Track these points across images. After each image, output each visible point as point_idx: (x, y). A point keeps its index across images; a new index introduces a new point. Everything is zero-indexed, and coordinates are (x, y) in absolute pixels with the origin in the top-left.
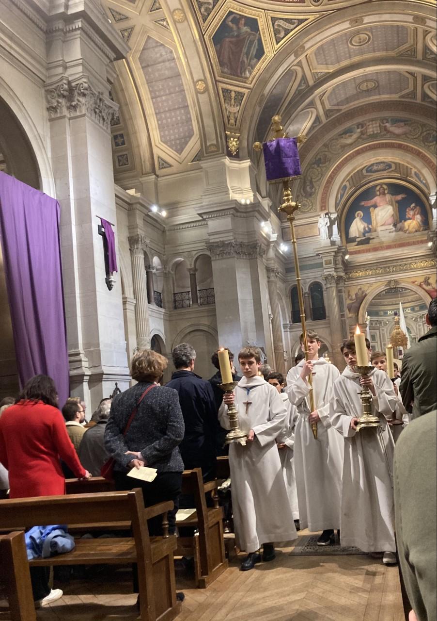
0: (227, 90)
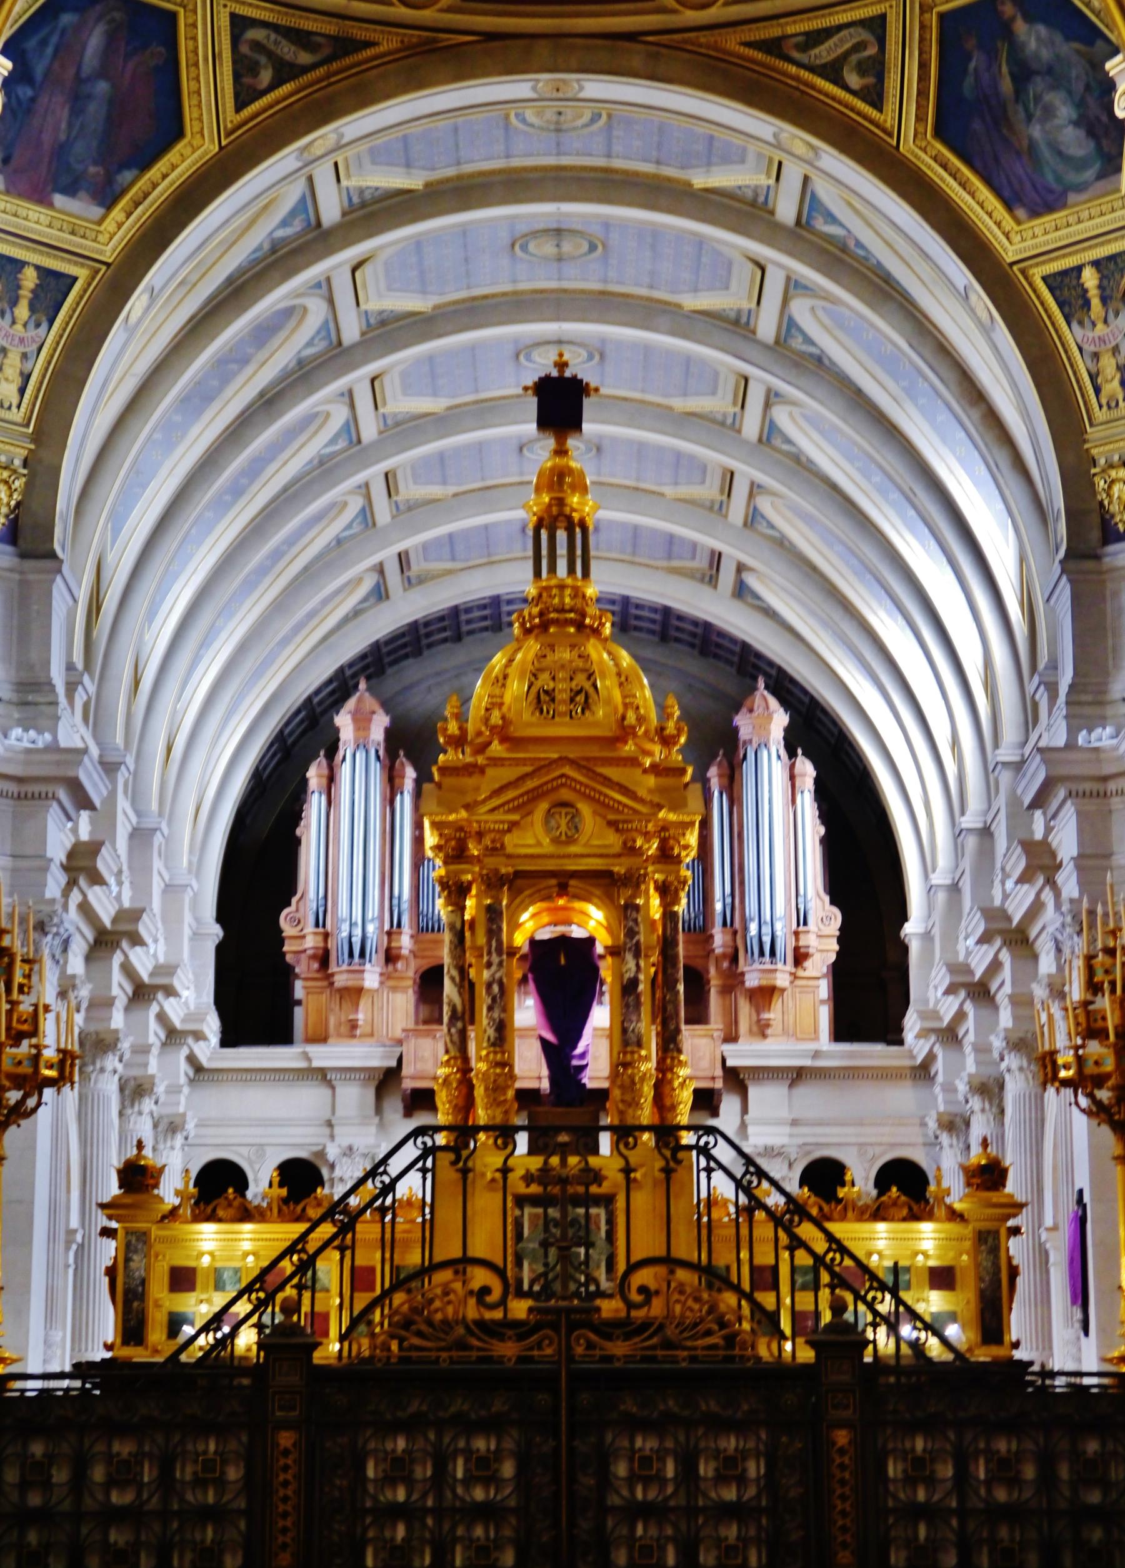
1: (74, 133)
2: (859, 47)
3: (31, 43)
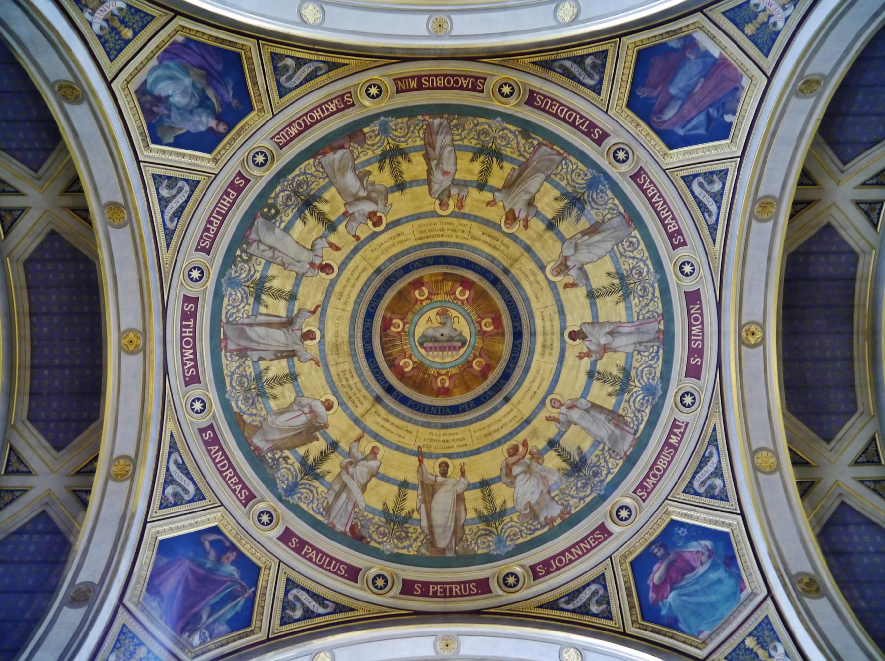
1: (696, 78)
2: (289, 78)
3: (702, 131)
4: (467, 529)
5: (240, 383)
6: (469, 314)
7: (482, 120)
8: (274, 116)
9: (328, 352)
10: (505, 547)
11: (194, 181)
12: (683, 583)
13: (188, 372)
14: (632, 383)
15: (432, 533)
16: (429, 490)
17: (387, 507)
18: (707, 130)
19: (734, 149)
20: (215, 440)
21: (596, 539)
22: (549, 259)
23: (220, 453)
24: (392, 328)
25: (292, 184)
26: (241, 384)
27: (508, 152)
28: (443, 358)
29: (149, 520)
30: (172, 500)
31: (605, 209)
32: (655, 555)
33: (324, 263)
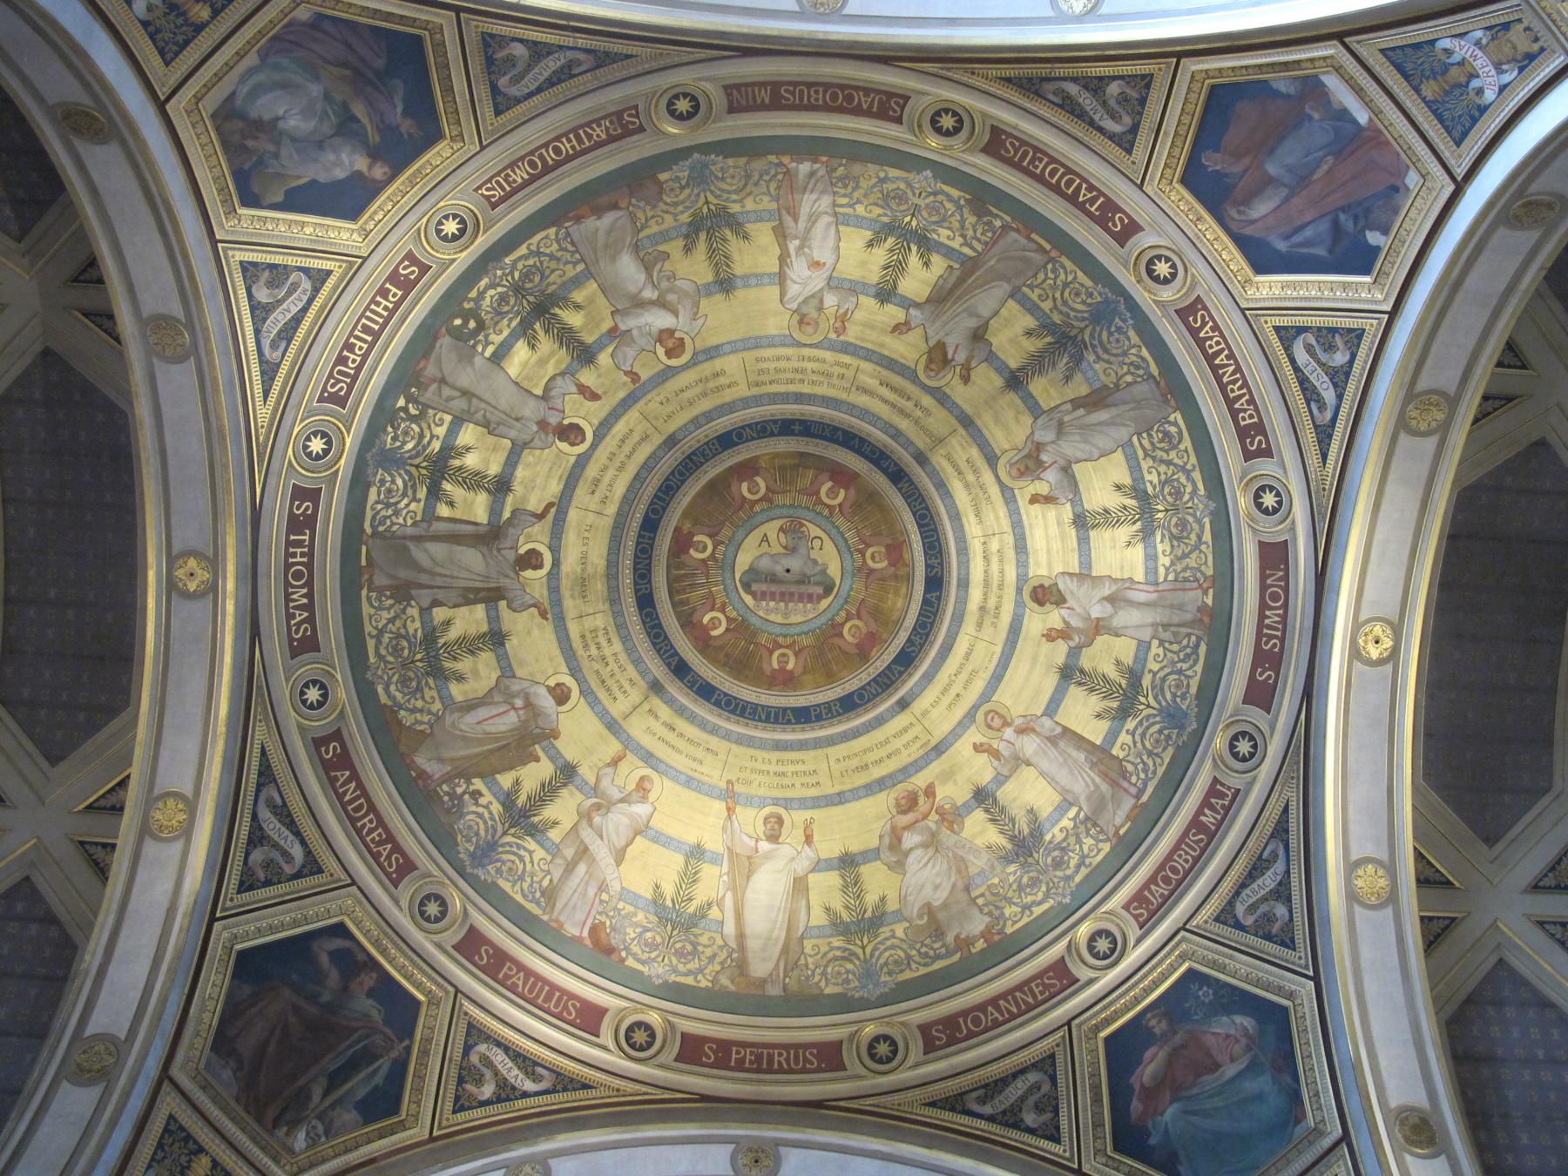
0: (189, 1137)
1: (1320, 154)
3: (1321, 251)
4: (808, 944)
5: (395, 649)
6: (842, 534)
7: (893, 173)
8: (483, 148)
9: (566, 592)
10: (877, 984)
11: (320, 270)
12: (1195, 1091)
13: (297, 632)
14: (1142, 700)
15: (742, 947)
16: (743, 867)
17: (661, 895)
18: (1331, 252)
19: (1380, 297)
20: (345, 760)
21: (1046, 987)
22: (1007, 446)
23: (353, 785)
24: (692, 551)
25: (512, 273)
26: (396, 651)
27: (943, 235)
28: (786, 615)
29: (218, 915)
30: (261, 875)
31: (1122, 364)
32: (1150, 1031)
33: (566, 422)
